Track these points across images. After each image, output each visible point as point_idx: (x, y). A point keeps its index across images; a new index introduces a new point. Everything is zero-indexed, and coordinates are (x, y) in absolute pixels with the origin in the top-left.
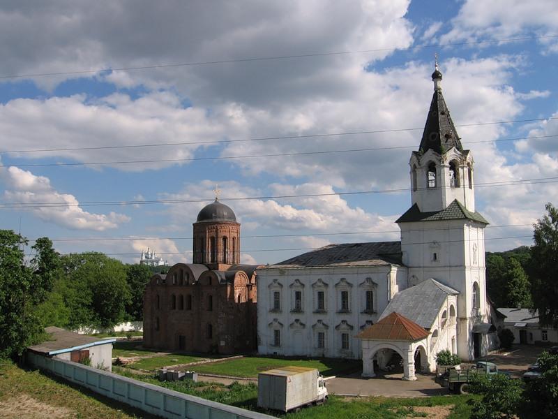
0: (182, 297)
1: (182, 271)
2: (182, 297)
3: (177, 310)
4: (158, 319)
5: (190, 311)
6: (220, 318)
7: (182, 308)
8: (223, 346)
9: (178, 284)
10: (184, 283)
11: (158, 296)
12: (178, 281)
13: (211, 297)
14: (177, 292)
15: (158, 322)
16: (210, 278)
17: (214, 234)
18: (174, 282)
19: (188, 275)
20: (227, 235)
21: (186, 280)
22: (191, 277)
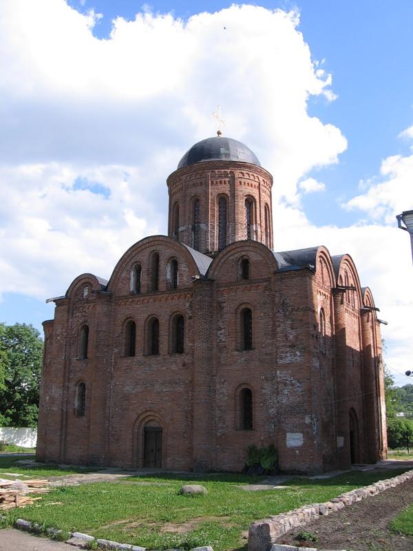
0: (154, 323)
1: (156, 258)
2: (154, 323)
3: (139, 355)
4: (83, 386)
5: (179, 358)
6: (286, 366)
7: (154, 350)
8: (293, 449)
9: (143, 290)
10: (162, 286)
11: (86, 329)
12: (145, 279)
13: (247, 314)
14: (141, 312)
15: (82, 397)
16: (245, 263)
17: (225, 189)
18: (132, 288)
19: (175, 264)
20: (255, 192)
21: (169, 276)
22: (183, 267)
